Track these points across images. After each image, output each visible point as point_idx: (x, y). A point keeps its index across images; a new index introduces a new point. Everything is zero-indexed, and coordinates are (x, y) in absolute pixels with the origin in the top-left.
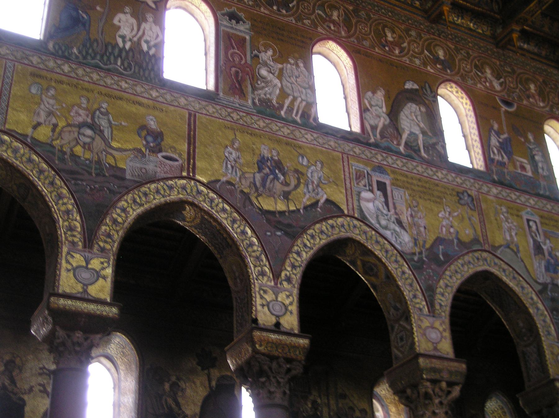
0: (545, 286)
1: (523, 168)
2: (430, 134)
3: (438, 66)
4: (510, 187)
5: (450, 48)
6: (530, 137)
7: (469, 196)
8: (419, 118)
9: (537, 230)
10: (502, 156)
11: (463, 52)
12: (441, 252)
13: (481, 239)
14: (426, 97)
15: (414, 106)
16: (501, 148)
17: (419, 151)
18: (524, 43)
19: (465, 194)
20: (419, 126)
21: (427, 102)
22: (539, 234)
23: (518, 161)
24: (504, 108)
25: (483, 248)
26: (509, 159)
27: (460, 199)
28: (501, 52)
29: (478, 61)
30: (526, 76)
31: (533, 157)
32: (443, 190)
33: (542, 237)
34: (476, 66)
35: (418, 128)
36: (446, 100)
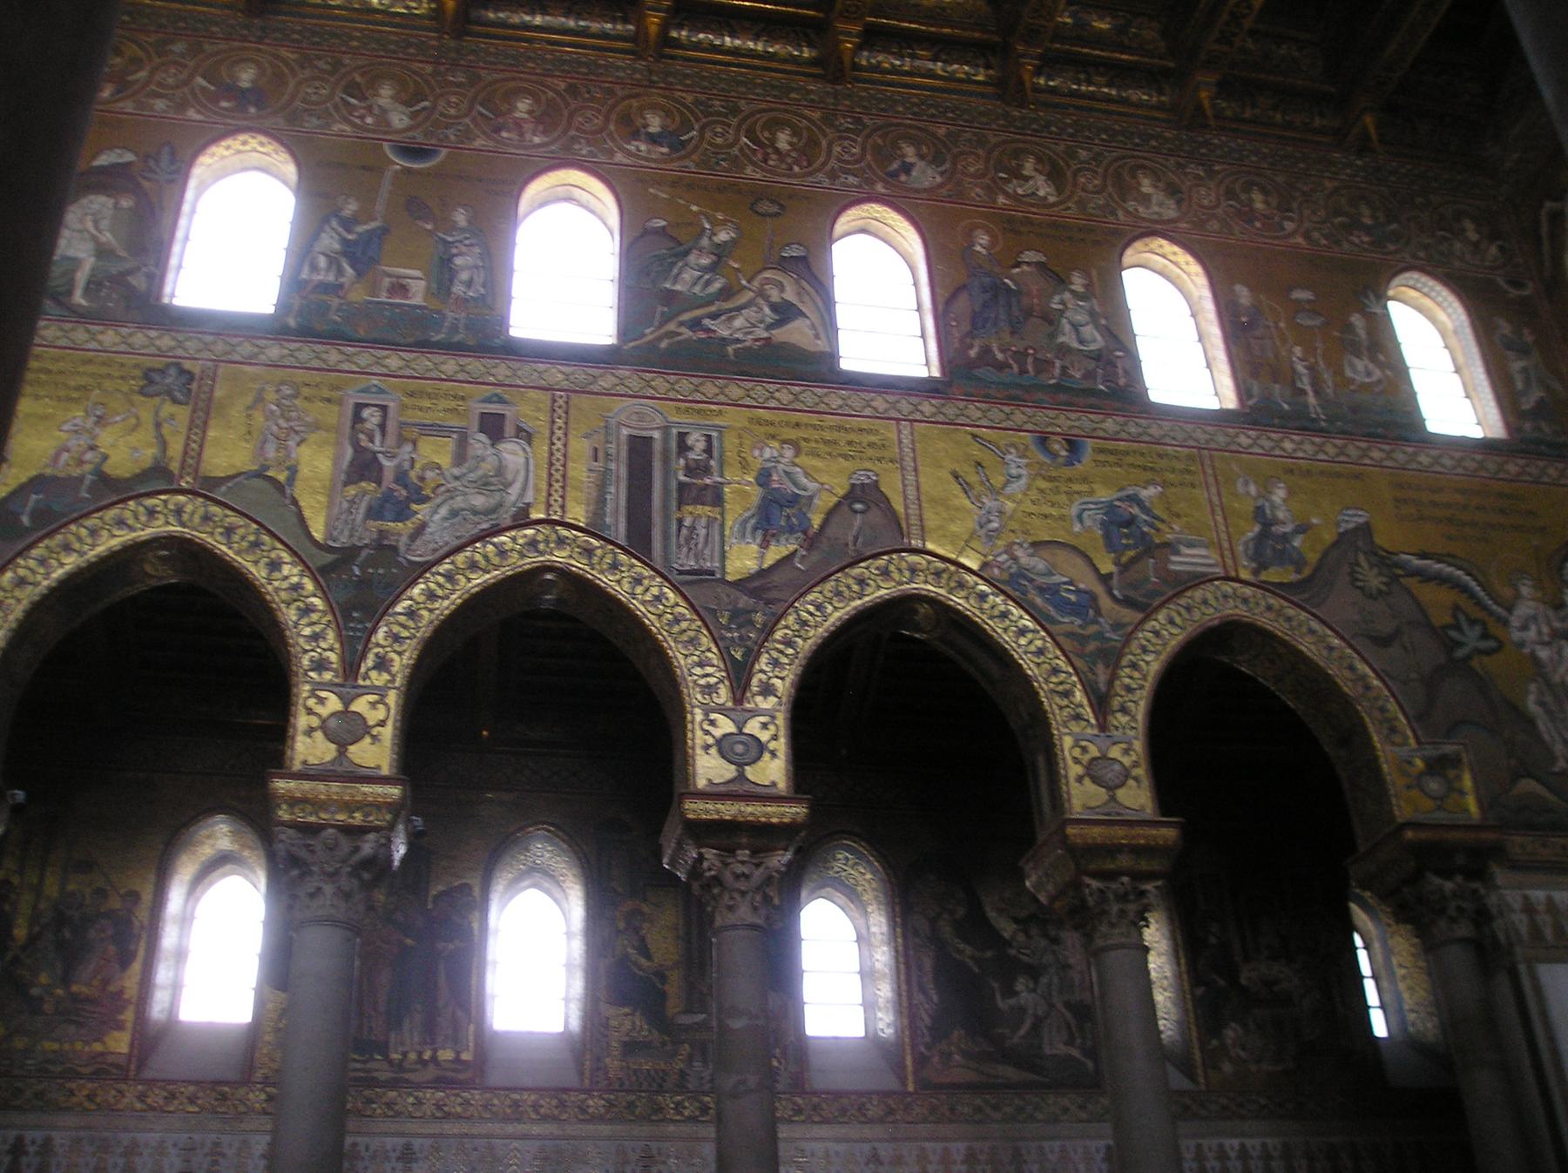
0: (348, 555)
1: (400, 288)
2: (123, 254)
3: (224, 104)
4: (335, 336)
5: (283, 60)
6: (461, 218)
7: (182, 371)
8: (104, 224)
9: (382, 427)
10: (340, 272)
11: (321, 64)
12: (28, 509)
13: (175, 466)
14: (147, 175)
15: (102, 199)
16: (345, 254)
17: (70, 293)
18: (533, 13)
19: (173, 371)
20: (94, 239)
21: (146, 184)
22: (384, 433)
23: (390, 276)
24: (400, 163)
25: (175, 486)
26: (359, 274)
27: (151, 382)
28: (453, 44)
29: (362, 75)
30: (512, 84)
31: (446, 263)
32: (104, 370)
33: (391, 439)
34: (353, 89)
35: (90, 246)
36: (276, 176)
